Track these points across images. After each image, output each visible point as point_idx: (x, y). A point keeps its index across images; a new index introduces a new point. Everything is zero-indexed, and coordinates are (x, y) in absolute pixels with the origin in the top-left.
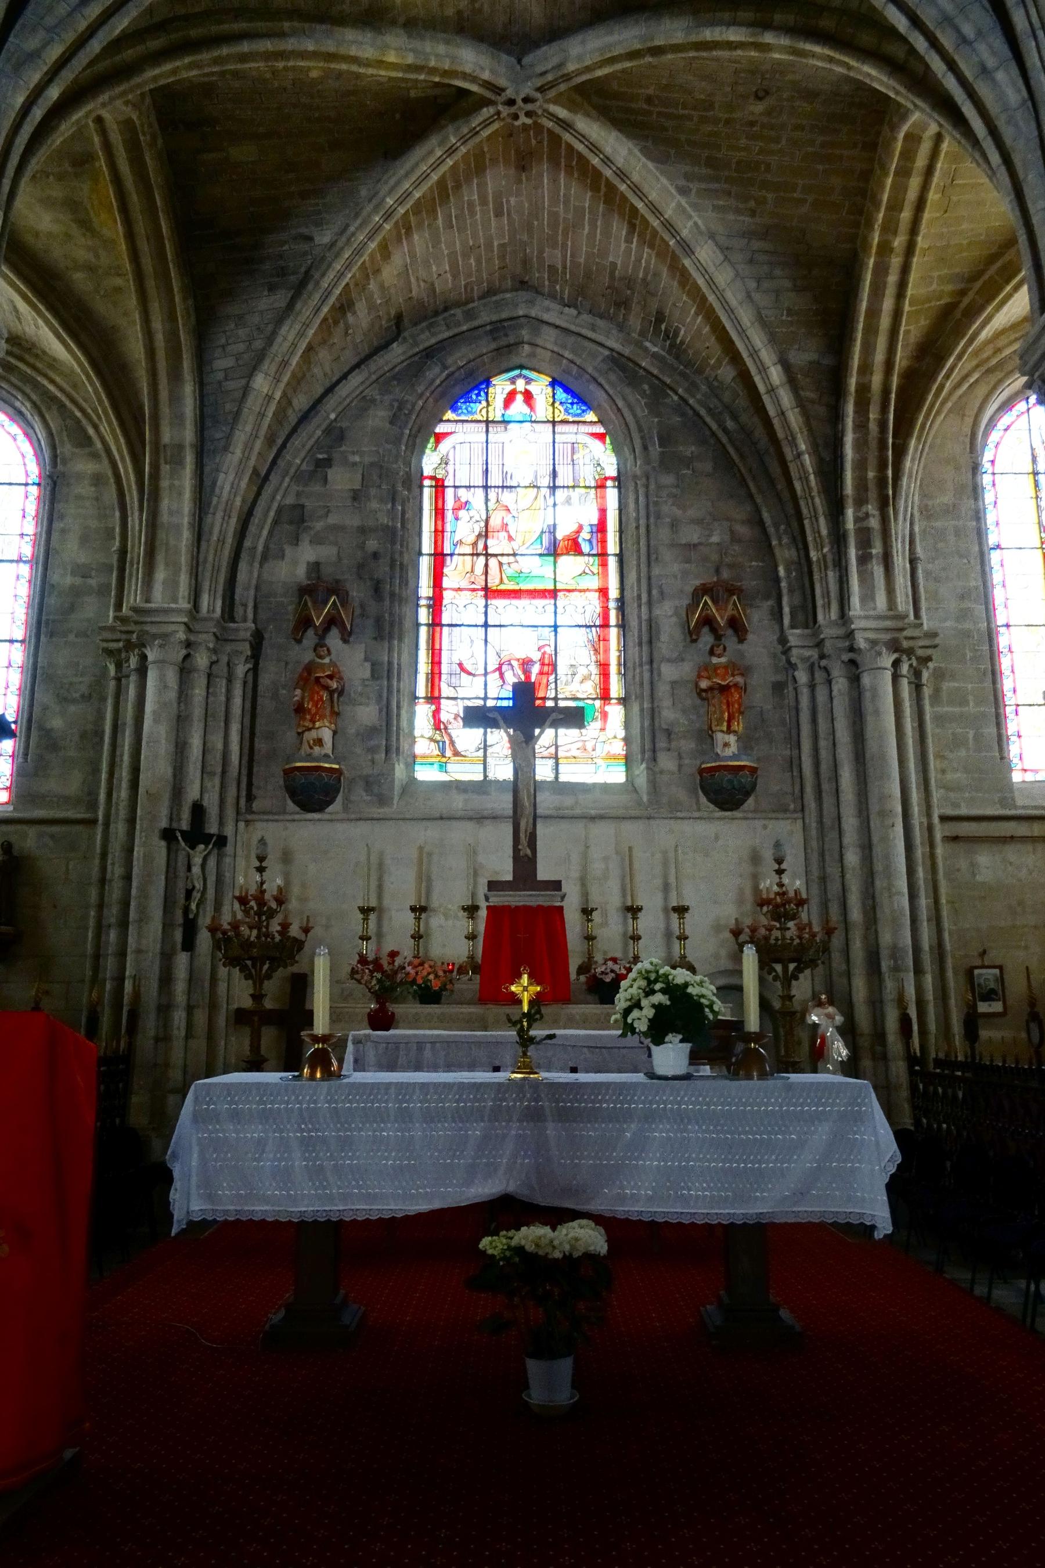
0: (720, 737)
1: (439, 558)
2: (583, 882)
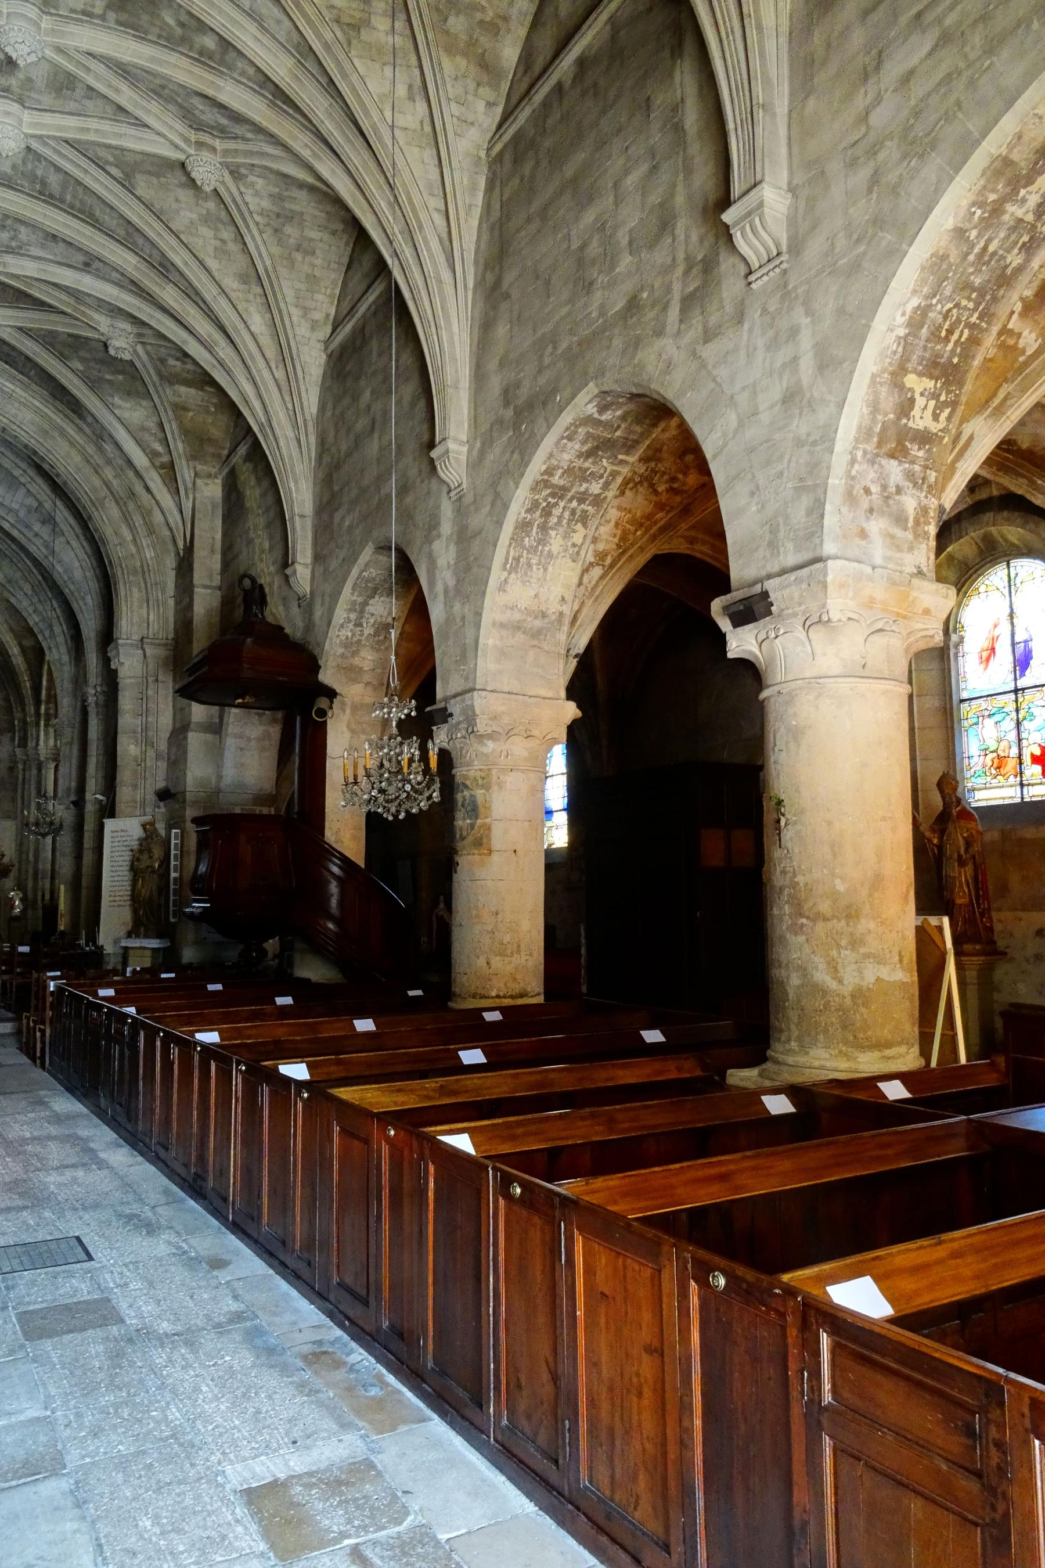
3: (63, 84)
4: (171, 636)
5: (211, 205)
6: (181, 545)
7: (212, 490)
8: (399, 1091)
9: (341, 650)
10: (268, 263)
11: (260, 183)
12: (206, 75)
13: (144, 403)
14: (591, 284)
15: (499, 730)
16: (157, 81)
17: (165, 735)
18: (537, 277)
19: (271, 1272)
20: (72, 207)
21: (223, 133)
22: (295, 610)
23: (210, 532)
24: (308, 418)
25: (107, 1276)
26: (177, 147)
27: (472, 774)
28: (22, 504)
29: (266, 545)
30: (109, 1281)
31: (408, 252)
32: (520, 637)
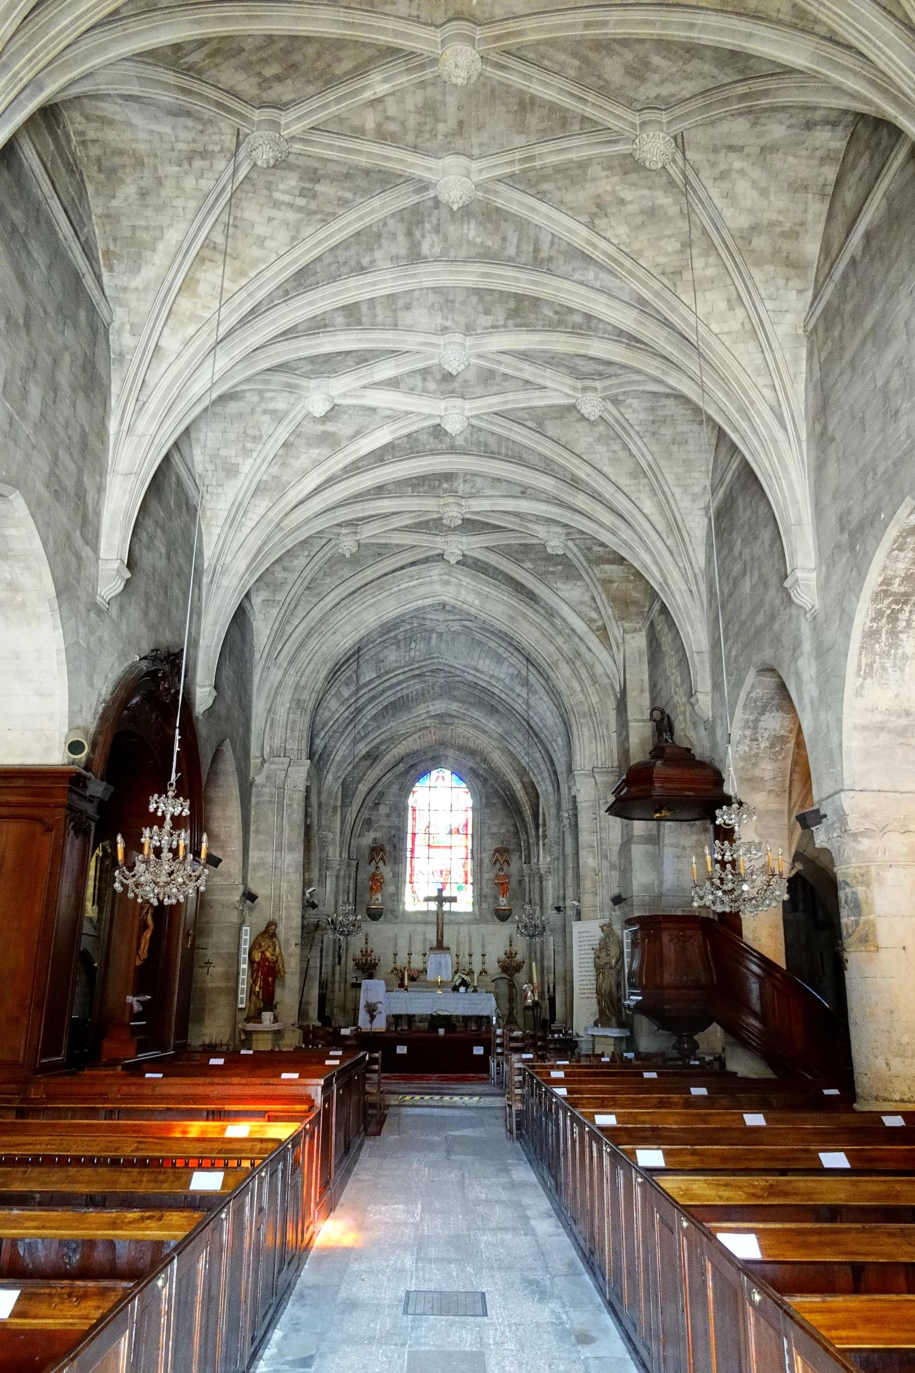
0: (501, 899)
1: (414, 834)
2: (458, 944)
3: (488, 378)
4: (616, 764)
5: (602, 428)
6: (618, 690)
7: (640, 641)
8: (726, 1185)
9: (741, 764)
10: (650, 458)
11: (635, 403)
12: (581, 341)
13: (579, 583)
14: (897, 412)
15: (873, 828)
16: (548, 355)
17: (616, 849)
18: (854, 417)
19: (628, 1356)
20: (506, 456)
21: (601, 376)
22: (703, 733)
23: (639, 675)
24: (697, 571)
25: (491, 1332)
26: (569, 396)
27: (851, 871)
28: (507, 674)
29: (679, 680)
30: (491, 1337)
31: (744, 425)
32: (885, 737)
